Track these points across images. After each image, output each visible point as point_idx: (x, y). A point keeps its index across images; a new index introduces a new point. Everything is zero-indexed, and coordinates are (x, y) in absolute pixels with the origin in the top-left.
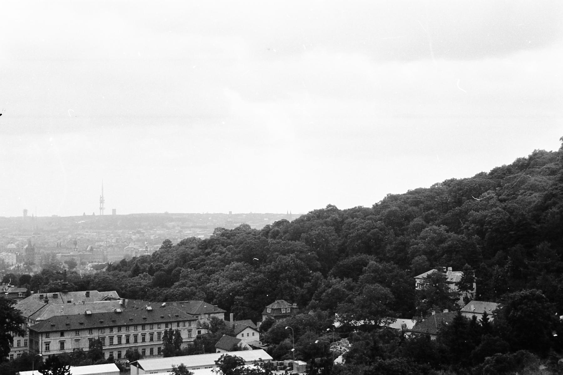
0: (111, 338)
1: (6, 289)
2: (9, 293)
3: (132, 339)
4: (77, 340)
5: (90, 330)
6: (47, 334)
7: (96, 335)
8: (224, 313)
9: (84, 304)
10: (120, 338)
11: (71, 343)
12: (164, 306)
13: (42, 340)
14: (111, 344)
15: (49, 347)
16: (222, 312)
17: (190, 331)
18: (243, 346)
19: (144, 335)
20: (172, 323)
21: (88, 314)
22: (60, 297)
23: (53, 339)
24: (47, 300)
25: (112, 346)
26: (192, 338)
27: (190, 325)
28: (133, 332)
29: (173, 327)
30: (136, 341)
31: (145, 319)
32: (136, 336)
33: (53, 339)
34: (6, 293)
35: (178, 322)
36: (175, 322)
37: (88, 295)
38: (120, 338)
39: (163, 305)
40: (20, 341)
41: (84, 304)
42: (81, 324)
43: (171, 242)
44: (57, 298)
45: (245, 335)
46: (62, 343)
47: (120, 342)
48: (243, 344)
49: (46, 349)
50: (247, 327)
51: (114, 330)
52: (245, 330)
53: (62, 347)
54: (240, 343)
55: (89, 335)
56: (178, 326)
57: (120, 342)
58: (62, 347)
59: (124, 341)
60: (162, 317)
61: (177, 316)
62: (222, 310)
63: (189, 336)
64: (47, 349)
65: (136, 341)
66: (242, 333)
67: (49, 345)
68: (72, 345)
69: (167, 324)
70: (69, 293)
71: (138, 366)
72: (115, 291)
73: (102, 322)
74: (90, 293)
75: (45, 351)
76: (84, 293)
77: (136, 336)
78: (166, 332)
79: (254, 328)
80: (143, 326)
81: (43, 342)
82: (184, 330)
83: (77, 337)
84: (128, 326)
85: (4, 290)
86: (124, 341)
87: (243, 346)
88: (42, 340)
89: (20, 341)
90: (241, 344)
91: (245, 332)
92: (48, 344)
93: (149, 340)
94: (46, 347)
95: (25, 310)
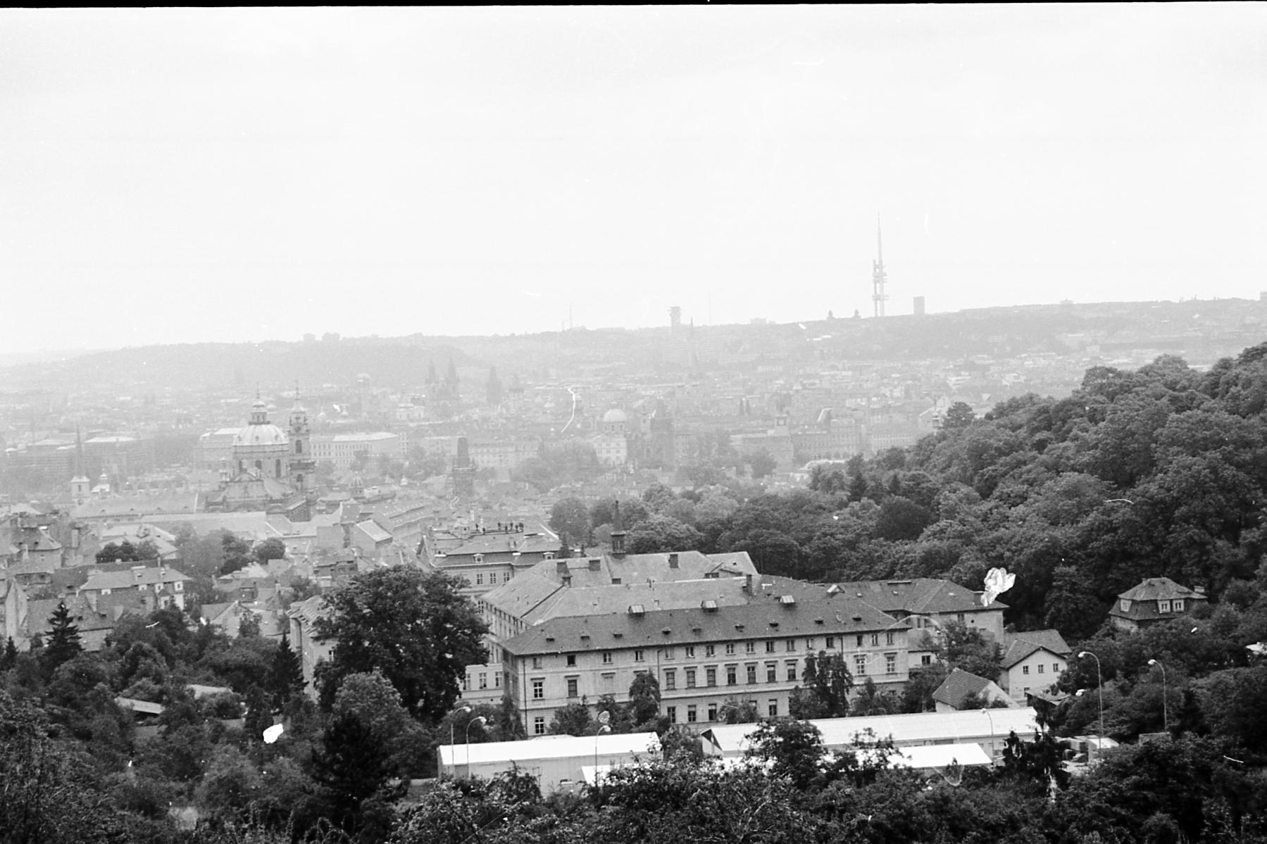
0: (691, 672)
1: (515, 544)
2: (522, 554)
3: (742, 675)
4: (608, 676)
5: (639, 651)
6: (535, 660)
7: (651, 663)
8: (1001, 614)
9: (650, 586)
10: (711, 671)
11: (595, 682)
12: (833, 594)
13: (526, 673)
14: (691, 685)
15: (541, 690)
16: (998, 609)
17: (891, 657)
18: (991, 699)
19: (771, 665)
20: (844, 638)
21: (637, 614)
22: (606, 568)
23: (552, 673)
24: (566, 576)
25: (694, 690)
26: (896, 674)
27: (890, 642)
28: (745, 657)
29: (847, 647)
30: (752, 680)
31: (774, 625)
32: (751, 669)
33: (552, 673)
34: (514, 554)
35: (859, 636)
36: (851, 634)
37: (673, 562)
38: (711, 671)
39: (830, 591)
40: (485, 674)
41: (650, 586)
42: (618, 636)
43: (971, 409)
44: (598, 569)
45: (1033, 669)
46: (573, 682)
47: (712, 683)
48: (990, 694)
49: (536, 696)
50: (1038, 650)
51: (696, 651)
52: (1031, 657)
53: (573, 691)
54: (984, 690)
55: (635, 664)
57: (712, 683)
58: (573, 691)
59: (722, 678)
60: (820, 622)
61: (858, 620)
63: (889, 670)
64: (538, 694)
65: (752, 680)
66: (1024, 664)
67: (540, 684)
68: (595, 689)
69: (830, 638)
70: (629, 556)
71: (712, 739)
72: (746, 553)
73: (667, 633)
74: (680, 559)
75: (533, 700)
76: (665, 557)
77: (751, 669)
78: (810, 661)
79: (1057, 652)
80: (770, 643)
81: (528, 678)
82: (876, 653)
83: (608, 669)
84: (730, 644)
85: (512, 547)
86: (722, 678)
87: (991, 699)
88: (526, 673)
89: (485, 674)
90: (987, 693)
91: (1032, 663)
92: (538, 684)
93: (787, 679)
94: (536, 690)
95: (518, 598)
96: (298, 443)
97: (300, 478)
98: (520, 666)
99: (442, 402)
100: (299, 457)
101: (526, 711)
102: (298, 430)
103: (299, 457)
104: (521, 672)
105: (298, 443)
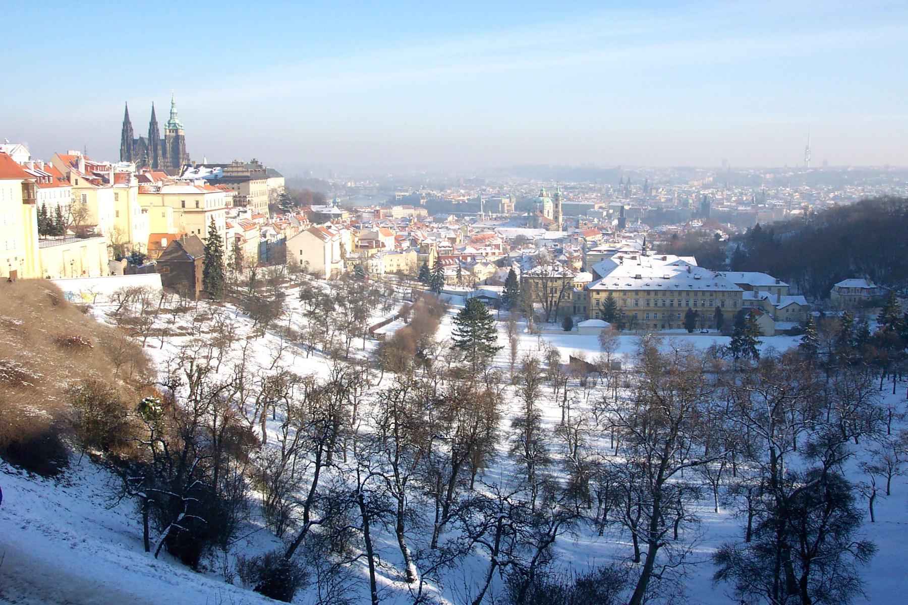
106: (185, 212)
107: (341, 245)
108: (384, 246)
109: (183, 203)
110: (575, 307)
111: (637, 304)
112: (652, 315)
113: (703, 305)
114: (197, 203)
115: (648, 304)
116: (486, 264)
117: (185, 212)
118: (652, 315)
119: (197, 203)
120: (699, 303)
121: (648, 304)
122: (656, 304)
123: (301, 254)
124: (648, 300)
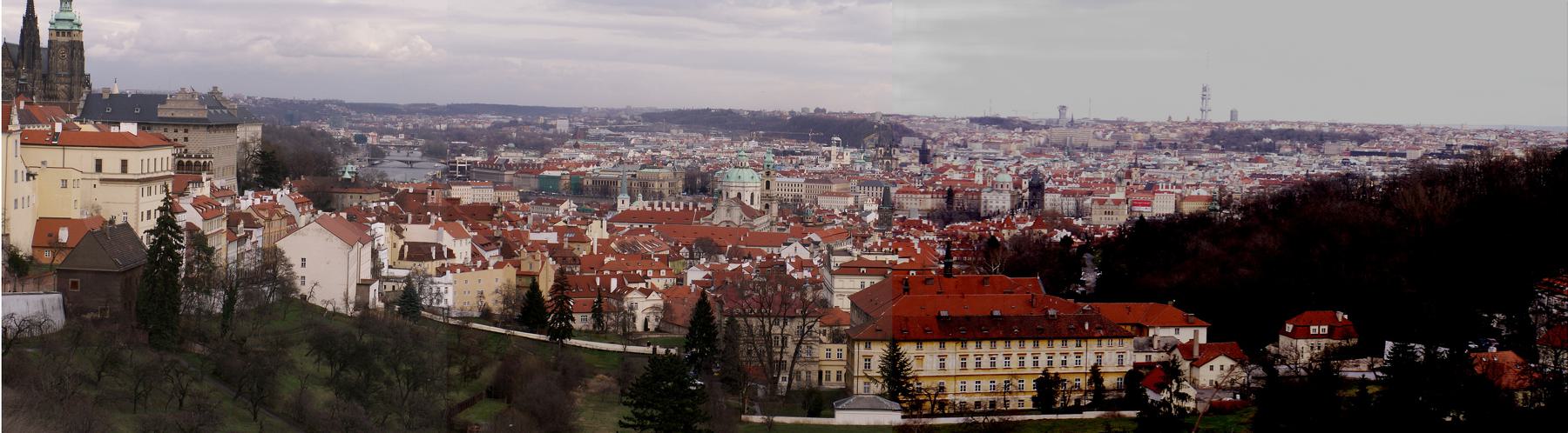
20: (1089, 342)
56: (1100, 345)
62: (1205, 323)
67: (869, 360)
96: (768, 183)
97: (767, 206)
98: (856, 347)
99: (885, 161)
100: (768, 192)
101: (858, 377)
102: (768, 174)
103: (768, 192)
104: (856, 351)
105: (768, 183)
106: (103, 181)
107: (375, 253)
108: (451, 254)
109: (99, 166)
110: (820, 373)
111: (942, 366)
112: (971, 385)
113: (1064, 363)
114: (124, 163)
115: (964, 365)
116: (646, 292)
117: (103, 181)
118: (971, 385)
119: (124, 163)
120: (1057, 360)
121: (964, 365)
122: (978, 365)
123: (303, 265)
124: (964, 357)
